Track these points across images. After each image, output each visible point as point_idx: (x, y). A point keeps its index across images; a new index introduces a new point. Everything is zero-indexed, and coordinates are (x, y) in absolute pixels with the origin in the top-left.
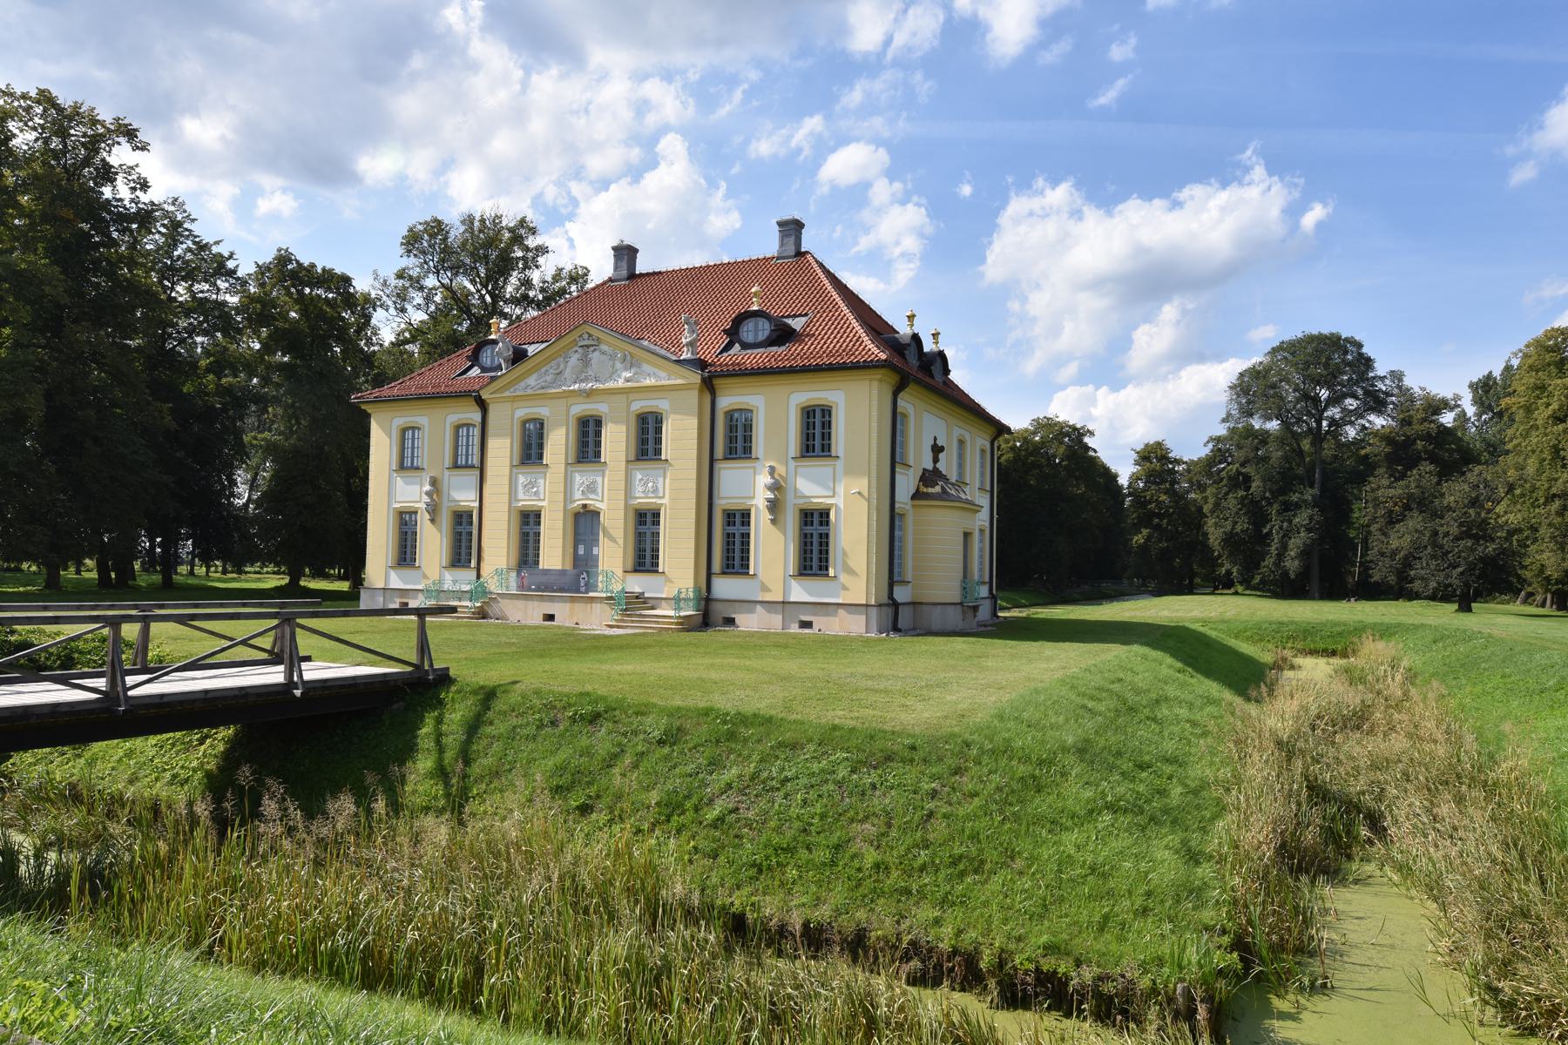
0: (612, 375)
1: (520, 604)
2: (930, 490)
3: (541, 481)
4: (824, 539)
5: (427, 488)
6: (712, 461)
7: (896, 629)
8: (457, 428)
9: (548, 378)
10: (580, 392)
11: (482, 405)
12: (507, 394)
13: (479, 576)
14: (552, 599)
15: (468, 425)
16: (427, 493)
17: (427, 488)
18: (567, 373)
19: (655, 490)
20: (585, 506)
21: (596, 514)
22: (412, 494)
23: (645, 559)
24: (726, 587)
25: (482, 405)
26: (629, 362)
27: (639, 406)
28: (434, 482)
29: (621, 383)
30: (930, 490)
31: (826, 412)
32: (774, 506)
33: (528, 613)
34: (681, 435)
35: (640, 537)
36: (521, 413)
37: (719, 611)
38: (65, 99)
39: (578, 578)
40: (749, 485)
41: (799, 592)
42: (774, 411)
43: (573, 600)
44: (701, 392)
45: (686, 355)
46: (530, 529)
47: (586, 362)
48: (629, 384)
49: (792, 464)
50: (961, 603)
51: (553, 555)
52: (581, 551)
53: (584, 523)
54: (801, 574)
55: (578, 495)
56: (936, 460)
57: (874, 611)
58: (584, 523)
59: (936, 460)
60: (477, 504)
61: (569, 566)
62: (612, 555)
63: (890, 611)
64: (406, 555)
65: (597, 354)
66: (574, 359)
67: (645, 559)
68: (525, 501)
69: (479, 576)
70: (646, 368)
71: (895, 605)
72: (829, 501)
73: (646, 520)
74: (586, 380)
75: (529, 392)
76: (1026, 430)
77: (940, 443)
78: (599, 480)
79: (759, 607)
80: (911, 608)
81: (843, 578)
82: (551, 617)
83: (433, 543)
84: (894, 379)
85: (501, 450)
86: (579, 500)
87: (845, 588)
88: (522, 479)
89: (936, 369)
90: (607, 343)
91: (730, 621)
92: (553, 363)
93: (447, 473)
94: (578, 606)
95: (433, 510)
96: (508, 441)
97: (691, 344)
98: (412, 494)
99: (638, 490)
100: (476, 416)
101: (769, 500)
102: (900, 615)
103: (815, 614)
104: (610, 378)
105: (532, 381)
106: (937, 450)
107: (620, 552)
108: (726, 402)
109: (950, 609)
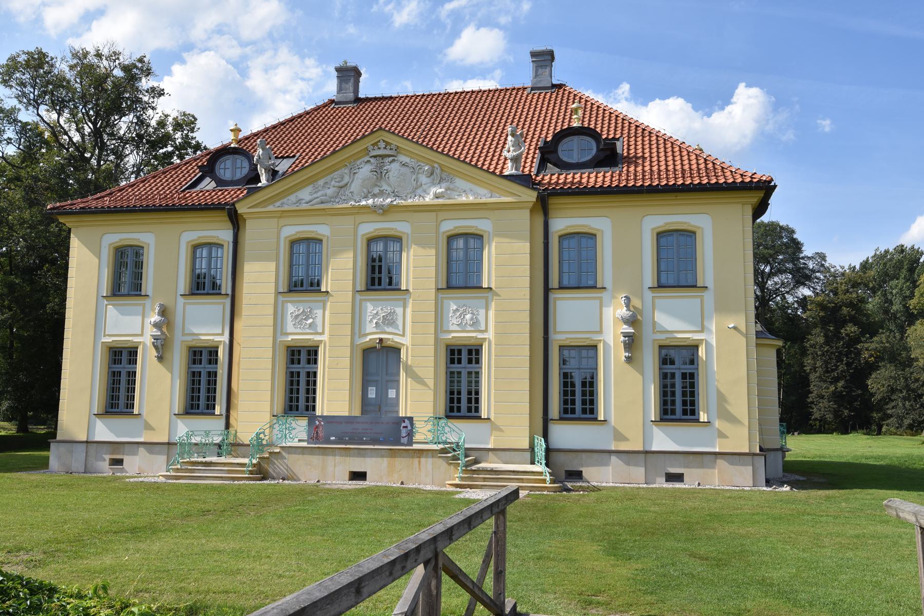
0: (417, 189)
1: (316, 459)
3: (319, 312)
4: (690, 379)
5: (155, 318)
6: (547, 290)
8: (196, 247)
9: (330, 192)
10: (374, 209)
12: (271, 208)
13: (228, 426)
14: (361, 453)
15: (210, 245)
16: (156, 325)
17: (155, 318)
18: (355, 187)
19: (475, 323)
20: (381, 340)
21: (394, 351)
22: (134, 325)
23: (461, 402)
24: (568, 435)
26: (438, 175)
27: (449, 226)
28: (163, 312)
29: (428, 199)
31: (690, 235)
32: (631, 342)
33: (332, 471)
34: (507, 261)
35: (452, 378)
36: (291, 231)
39: (380, 427)
40: (601, 320)
41: (663, 440)
42: (623, 237)
43: (393, 454)
44: (532, 211)
45: (509, 170)
46: (303, 368)
47: (380, 174)
48: (440, 201)
49: (649, 295)
51: (335, 396)
52: (372, 393)
53: (378, 362)
54: (662, 420)
55: (370, 327)
58: (378, 362)
60: (226, 338)
61: (357, 412)
62: (417, 398)
64: (119, 397)
65: (395, 166)
66: (365, 171)
67: (461, 402)
68: (296, 334)
69: (228, 426)
70: (460, 183)
72: (697, 337)
73: (462, 359)
74: (382, 193)
75: (304, 206)
78: (399, 311)
79: (614, 458)
81: (717, 424)
82: (359, 476)
83: (159, 387)
85: (260, 278)
86: (371, 334)
87: (721, 435)
88: (291, 309)
90: (408, 153)
91: (577, 475)
92: (336, 175)
93: (181, 301)
94: (400, 462)
95: (162, 347)
96: (272, 266)
97: (516, 160)
98: (134, 325)
99: (453, 323)
100: (225, 235)
101: (626, 335)
103: (685, 467)
104: (414, 192)
105: (305, 194)
107: (429, 395)
108: (561, 224)
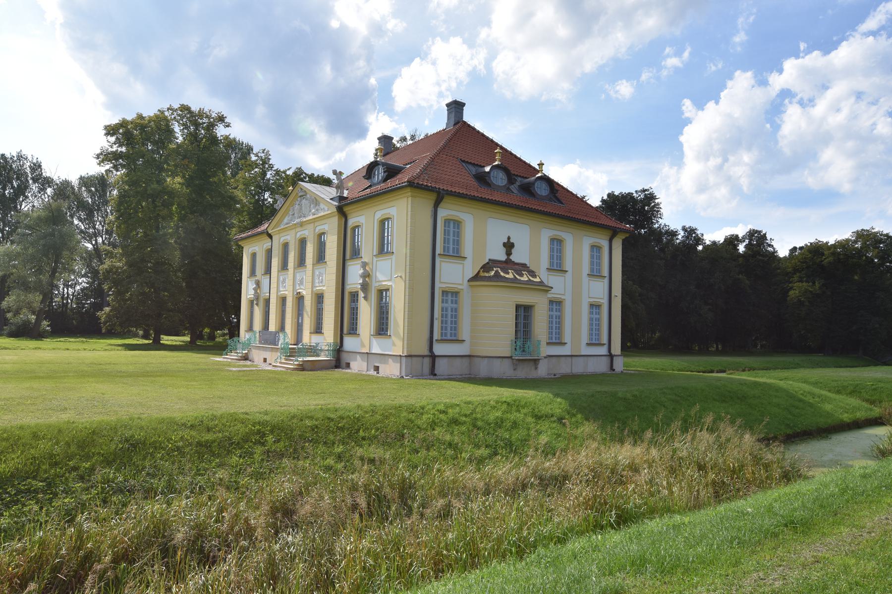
2: (487, 275)
7: (433, 373)
11: (270, 236)
25: (270, 236)
29: (311, 217)
30: (487, 275)
37: (345, 358)
38: (195, 108)
50: (511, 357)
56: (509, 253)
57: (404, 359)
59: (509, 253)
63: (427, 361)
68: (283, 292)
71: (433, 357)
72: (389, 283)
76: (847, 240)
77: (512, 241)
80: (465, 360)
81: (393, 338)
84: (433, 196)
87: (394, 344)
89: (542, 190)
91: (348, 366)
102: (427, 364)
106: (509, 246)
109: (497, 362)
